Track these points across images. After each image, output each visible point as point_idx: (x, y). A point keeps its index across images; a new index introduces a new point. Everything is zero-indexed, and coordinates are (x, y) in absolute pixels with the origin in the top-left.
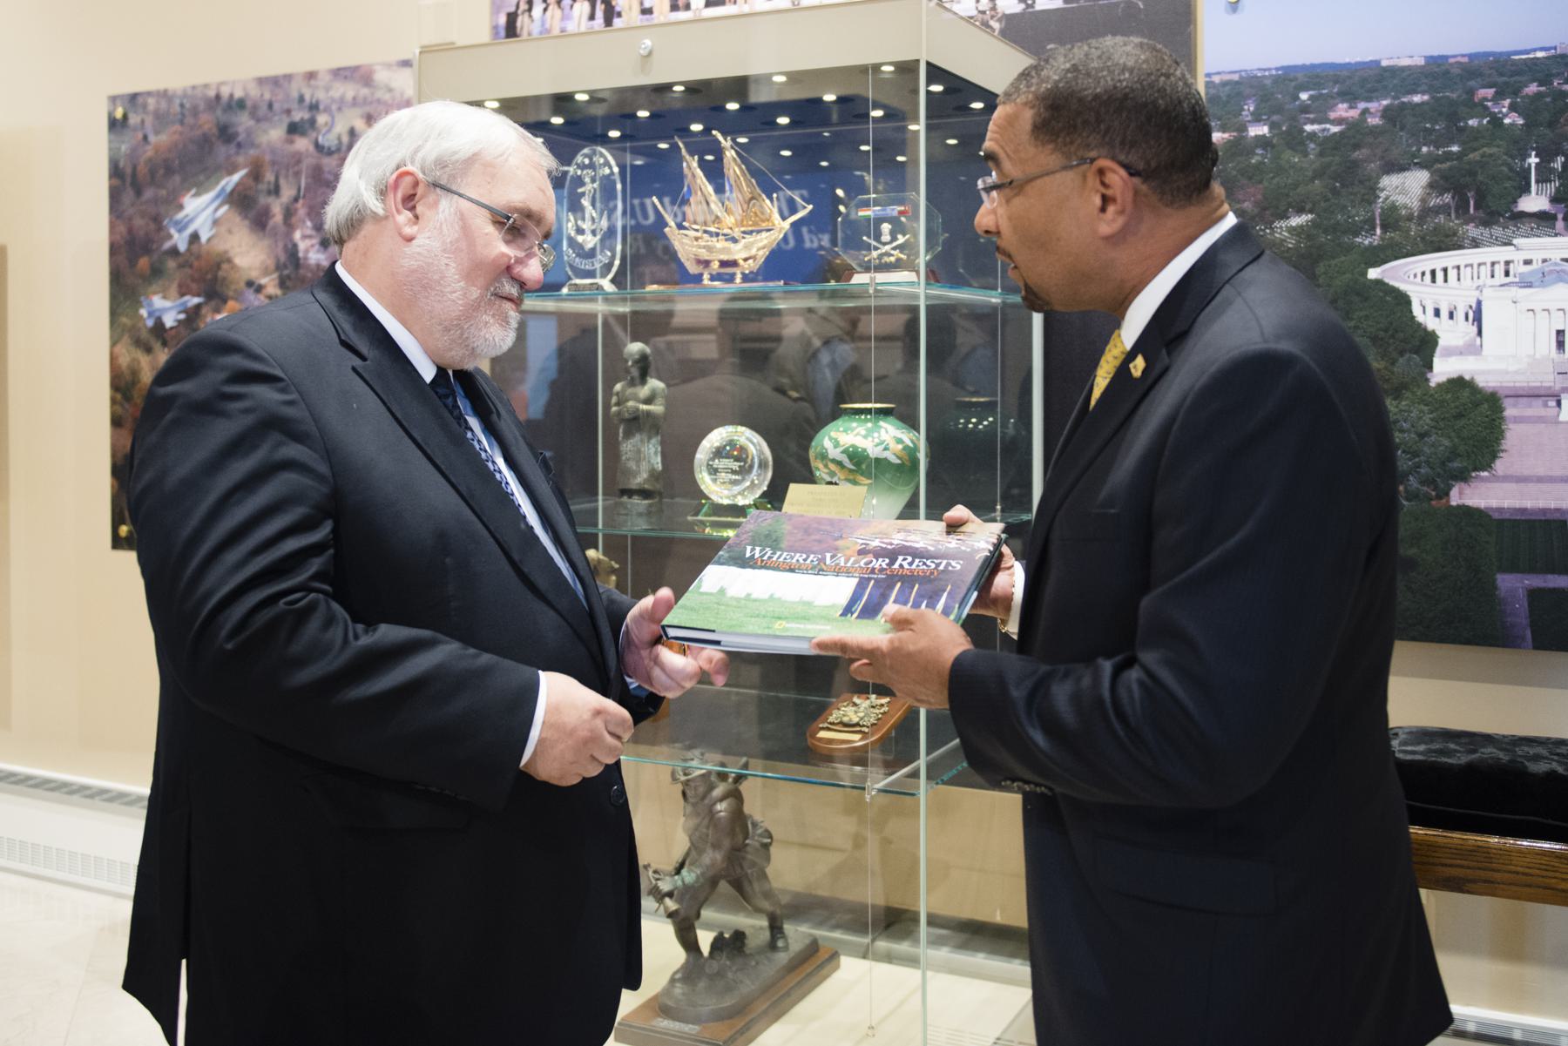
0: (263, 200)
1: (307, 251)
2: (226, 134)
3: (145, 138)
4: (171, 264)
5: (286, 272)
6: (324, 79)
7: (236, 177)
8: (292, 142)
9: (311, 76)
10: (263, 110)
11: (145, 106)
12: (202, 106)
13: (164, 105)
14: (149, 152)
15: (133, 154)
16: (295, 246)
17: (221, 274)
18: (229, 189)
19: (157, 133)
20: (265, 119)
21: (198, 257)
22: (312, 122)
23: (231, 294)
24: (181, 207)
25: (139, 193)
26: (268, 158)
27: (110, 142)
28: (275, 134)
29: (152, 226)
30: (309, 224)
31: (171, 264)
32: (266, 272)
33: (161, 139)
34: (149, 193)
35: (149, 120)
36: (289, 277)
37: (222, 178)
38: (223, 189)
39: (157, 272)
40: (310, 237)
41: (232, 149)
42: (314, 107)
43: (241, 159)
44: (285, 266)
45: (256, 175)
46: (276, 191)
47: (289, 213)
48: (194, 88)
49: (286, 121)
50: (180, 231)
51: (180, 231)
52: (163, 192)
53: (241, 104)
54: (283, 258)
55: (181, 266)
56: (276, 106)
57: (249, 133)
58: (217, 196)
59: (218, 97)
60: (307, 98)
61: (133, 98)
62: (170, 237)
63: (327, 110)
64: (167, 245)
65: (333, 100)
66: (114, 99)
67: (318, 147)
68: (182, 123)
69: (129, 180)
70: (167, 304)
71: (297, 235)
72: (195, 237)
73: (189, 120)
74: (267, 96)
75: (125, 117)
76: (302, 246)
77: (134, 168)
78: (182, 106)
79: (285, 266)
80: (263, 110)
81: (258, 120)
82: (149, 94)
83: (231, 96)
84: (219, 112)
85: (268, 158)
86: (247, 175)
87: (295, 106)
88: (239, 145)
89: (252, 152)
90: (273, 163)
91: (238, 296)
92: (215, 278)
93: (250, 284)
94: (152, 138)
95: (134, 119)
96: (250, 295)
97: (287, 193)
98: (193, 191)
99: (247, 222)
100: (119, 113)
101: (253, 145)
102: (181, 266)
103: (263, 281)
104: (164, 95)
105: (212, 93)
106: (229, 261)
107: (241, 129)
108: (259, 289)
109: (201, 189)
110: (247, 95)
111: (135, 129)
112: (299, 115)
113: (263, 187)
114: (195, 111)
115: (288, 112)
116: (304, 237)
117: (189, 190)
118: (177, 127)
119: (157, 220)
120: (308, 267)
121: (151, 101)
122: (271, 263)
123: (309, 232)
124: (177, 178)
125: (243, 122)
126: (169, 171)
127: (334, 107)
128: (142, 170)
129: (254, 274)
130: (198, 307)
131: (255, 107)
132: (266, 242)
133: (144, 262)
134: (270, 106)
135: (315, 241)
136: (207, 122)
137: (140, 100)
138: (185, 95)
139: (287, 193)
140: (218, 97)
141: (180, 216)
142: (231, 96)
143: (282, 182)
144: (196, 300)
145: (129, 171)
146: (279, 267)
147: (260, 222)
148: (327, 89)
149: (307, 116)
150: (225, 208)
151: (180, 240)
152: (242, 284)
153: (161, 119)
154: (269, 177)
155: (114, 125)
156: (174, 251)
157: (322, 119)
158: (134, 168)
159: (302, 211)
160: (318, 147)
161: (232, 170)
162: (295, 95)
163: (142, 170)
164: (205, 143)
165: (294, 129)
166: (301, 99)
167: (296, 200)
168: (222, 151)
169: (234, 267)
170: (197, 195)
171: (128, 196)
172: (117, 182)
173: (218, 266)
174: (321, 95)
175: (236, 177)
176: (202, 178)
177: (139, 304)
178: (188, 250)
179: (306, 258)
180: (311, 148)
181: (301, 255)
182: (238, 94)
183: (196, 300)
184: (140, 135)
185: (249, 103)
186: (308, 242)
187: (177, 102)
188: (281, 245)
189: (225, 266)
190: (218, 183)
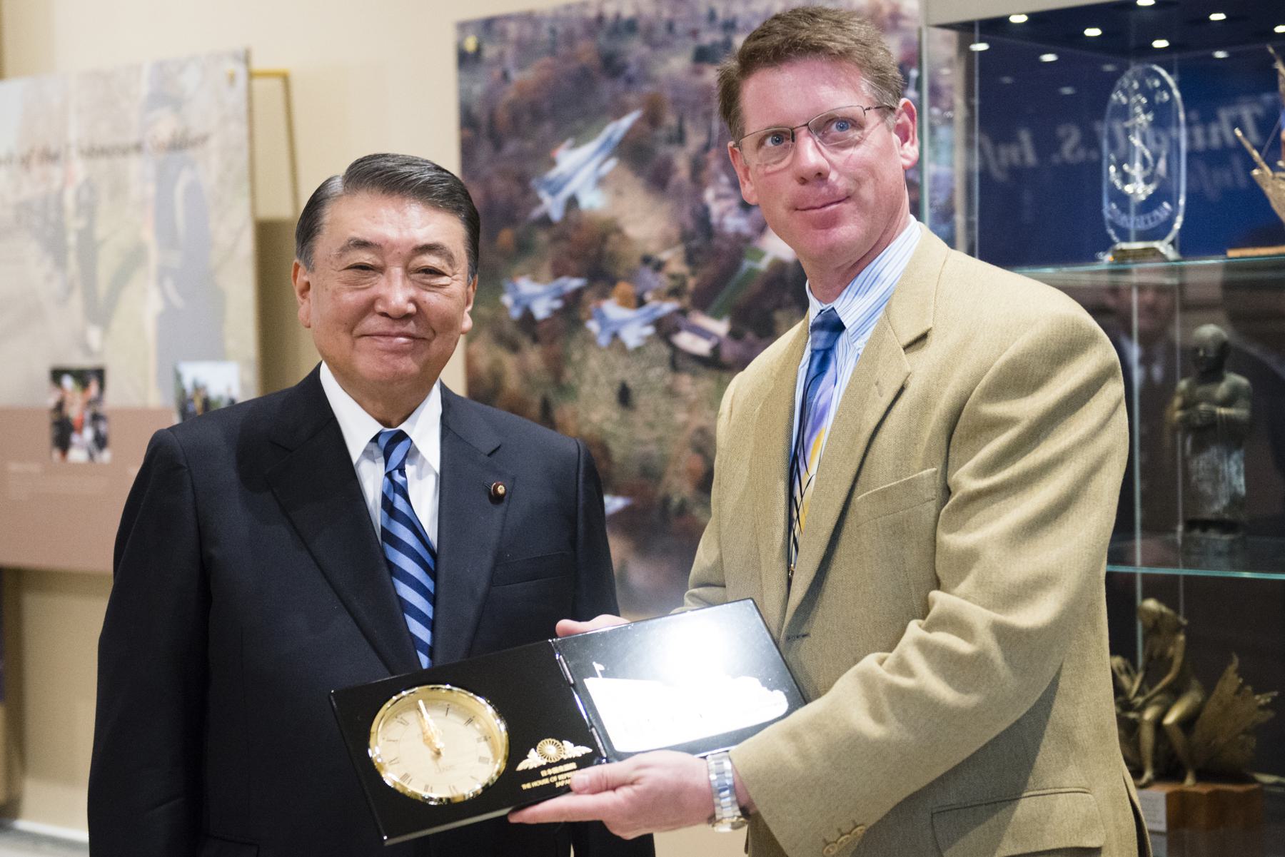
0: (663, 150)
1: (722, 215)
2: (612, 66)
3: (505, 76)
4: (542, 237)
5: (695, 243)
7: (626, 122)
8: (699, 72)
10: (661, 33)
11: (503, 33)
12: (579, 30)
13: (528, 31)
14: (510, 94)
15: (489, 98)
16: (706, 209)
17: (609, 248)
18: (617, 137)
19: (521, 66)
20: (665, 44)
21: (578, 227)
23: (621, 272)
24: (553, 163)
25: (498, 144)
26: (668, 95)
27: (461, 81)
28: (677, 64)
29: (517, 190)
30: (724, 179)
31: (542, 237)
32: (667, 244)
33: (525, 76)
34: (511, 147)
35: (510, 52)
36: (698, 250)
37: (607, 123)
38: (609, 139)
39: (523, 248)
40: (726, 197)
41: (620, 85)
43: (632, 98)
44: (693, 236)
45: (652, 118)
46: (679, 138)
47: (697, 167)
48: (568, 7)
49: (691, 45)
50: (554, 193)
51: (554, 193)
52: (530, 145)
53: (631, 26)
54: (690, 224)
55: (555, 240)
56: (679, 27)
57: (643, 63)
58: (602, 147)
59: (600, 19)
60: (720, 14)
61: (488, 26)
62: (539, 202)
64: (537, 213)
66: (463, 27)
68: (552, 52)
69: (484, 130)
70: (536, 288)
71: (709, 195)
72: (572, 202)
73: (563, 50)
74: (666, 13)
75: (479, 50)
76: (716, 208)
77: (492, 115)
78: (553, 31)
79: (693, 236)
80: (661, 33)
81: (655, 46)
82: (508, 18)
83: (618, 16)
84: (602, 39)
85: (668, 95)
86: (640, 120)
87: (702, 25)
88: (630, 81)
89: (648, 88)
90: (676, 102)
91: (631, 277)
92: (600, 256)
93: (647, 260)
94: (516, 76)
95: (490, 52)
96: (647, 275)
97: (695, 140)
98: (569, 142)
99: (640, 181)
100: (471, 44)
101: (648, 79)
102: (555, 240)
103: (665, 256)
104: (529, 18)
105: (591, 13)
106: (619, 231)
107: (631, 59)
108: (659, 266)
109: (580, 138)
110: (640, 14)
111: (492, 64)
112: (709, 37)
113: (662, 133)
114: (570, 38)
115: (694, 33)
116: (719, 197)
117: (563, 140)
118: (547, 60)
119: (523, 181)
120: (723, 236)
121: (513, 29)
122: (674, 232)
123: (725, 190)
124: (547, 127)
125: (635, 49)
126: (537, 115)
128: (503, 116)
129: (652, 248)
130: (578, 293)
131: (650, 30)
132: (667, 206)
133: (506, 236)
134: (670, 27)
135: (733, 202)
136: (586, 51)
137: (497, 27)
138: (556, 18)
139: (695, 140)
140: (600, 19)
141: (553, 174)
142: (618, 16)
143: (688, 126)
144: (575, 283)
145: (484, 119)
146: (685, 237)
147: (659, 180)
150: (612, 164)
151: (553, 206)
152: (635, 262)
153: (526, 49)
154: (670, 120)
155: (466, 60)
156: (546, 221)
158: (492, 115)
159: (714, 164)
161: (620, 112)
162: (703, 10)
163: (503, 116)
164: (583, 81)
165: (703, 56)
166: (712, 16)
167: (706, 148)
168: (606, 89)
169: (625, 239)
170: (576, 146)
171: (484, 152)
172: (469, 133)
173: (604, 238)
175: (626, 122)
176: (580, 124)
177: (500, 290)
178: (566, 218)
179: (721, 225)
181: (714, 220)
182: (628, 12)
183: (575, 283)
184: (497, 72)
185: (642, 24)
186: (724, 204)
187: (546, 26)
188: (687, 209)
189: (614, 238)
190: (600, 130)
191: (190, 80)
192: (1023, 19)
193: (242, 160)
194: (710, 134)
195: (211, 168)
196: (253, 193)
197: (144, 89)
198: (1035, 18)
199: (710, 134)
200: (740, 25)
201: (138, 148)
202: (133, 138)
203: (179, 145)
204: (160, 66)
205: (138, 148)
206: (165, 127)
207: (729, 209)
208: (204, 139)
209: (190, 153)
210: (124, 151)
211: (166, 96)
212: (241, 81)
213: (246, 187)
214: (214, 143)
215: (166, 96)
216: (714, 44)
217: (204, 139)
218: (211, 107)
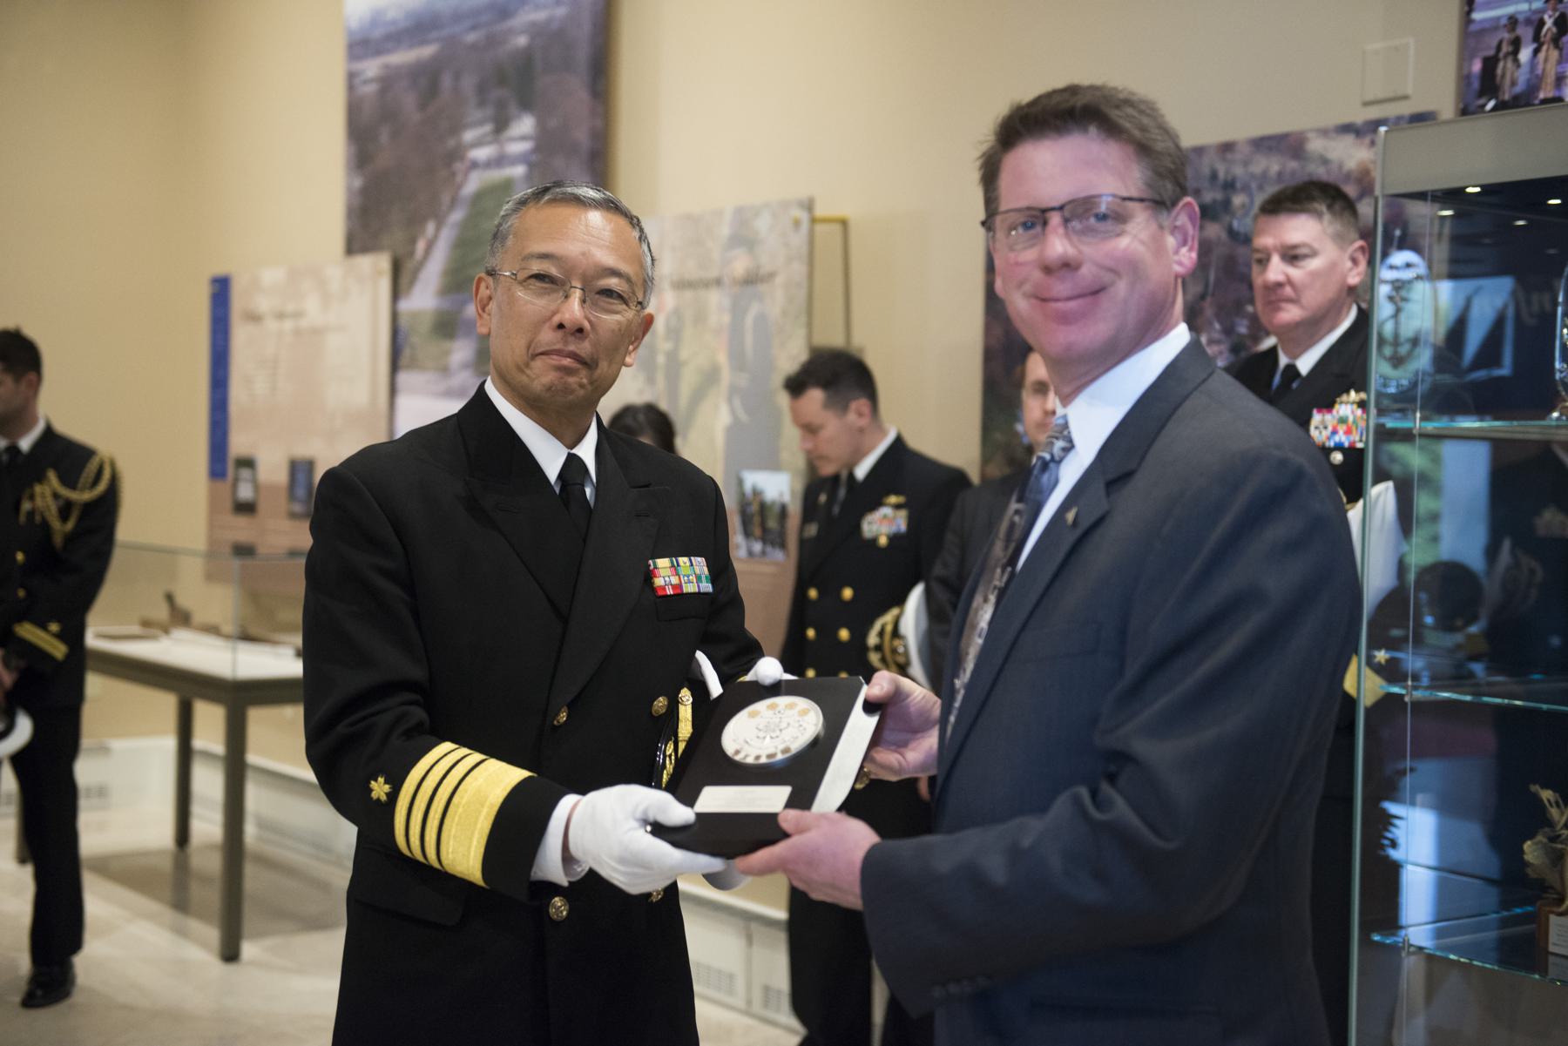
6: (1243, 151)
9: (1227, 148)
22: (1227, 204)
30: (1217, 326)
40: (1218, 342)
42: (1230, 186)
60: (1221, 175)
63: (1246, 189)
65: (1253, 176)
67: (1231, 232)
112: (1209, 196)
116: (1211, 342)
123: (1216, 336)
127: (1254, 185)
135: (1224, 347)
148: (1246, 164)
149: (1218, 196)
157: (1238, 200)
159: (1209, 310)
160: (1231, 232)
162: (1206, 171)
166: (1214, 176)
167: (1203, 297)
174: (1238, 171)
180: (1224, 235)
191: (763, 224)
192: (1478, 190)
193: (802, 294)
194: (1207, 285)
195: (775, 302)
196: (810, 325)
197: (725, 231)
198: (1487, 189)
199: (1207, 285)
200: (1238, 185)
201: (718, 282)
202: (713, 273)
203: (752, 280)
204: (739, 211)
205: (718, 282)
206: (740, 265)
207: (1221, 353)
208: (771, 276)
209: (762, 288)
210: (706, 284)
211: (743, 238)
212: (805, 225)
213: (803, 319)
214: (779, 280)
215: (743, 238)
216: (1215, 202)
217: (771, 276)
218: (778, 249)
